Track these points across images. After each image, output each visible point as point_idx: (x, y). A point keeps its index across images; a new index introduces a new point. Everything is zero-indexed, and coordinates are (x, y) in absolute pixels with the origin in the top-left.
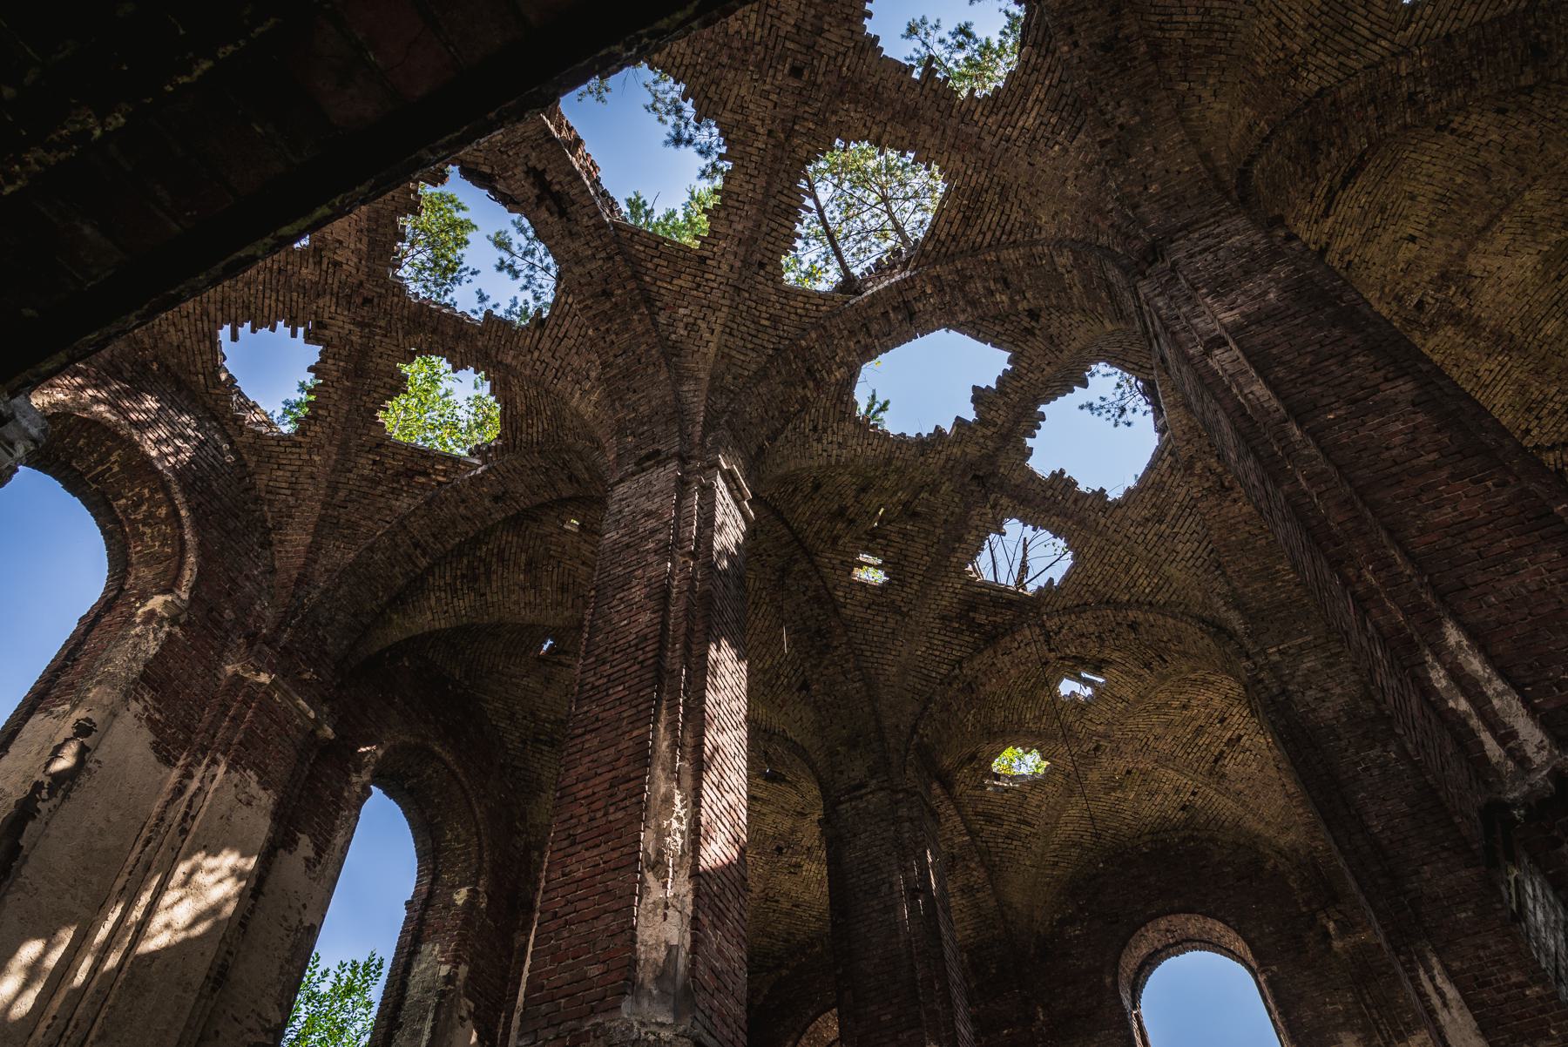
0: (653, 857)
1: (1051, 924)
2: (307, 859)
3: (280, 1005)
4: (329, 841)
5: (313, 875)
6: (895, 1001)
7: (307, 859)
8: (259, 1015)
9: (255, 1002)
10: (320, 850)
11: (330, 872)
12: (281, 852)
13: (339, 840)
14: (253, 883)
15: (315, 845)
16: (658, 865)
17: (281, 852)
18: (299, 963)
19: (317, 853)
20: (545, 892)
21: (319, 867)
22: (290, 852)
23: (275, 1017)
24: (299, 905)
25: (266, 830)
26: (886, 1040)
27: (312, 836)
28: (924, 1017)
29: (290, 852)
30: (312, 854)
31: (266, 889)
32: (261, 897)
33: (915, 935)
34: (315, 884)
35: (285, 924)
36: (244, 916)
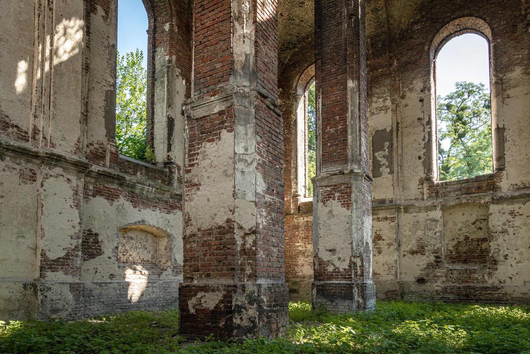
0: (237, 14)
1: (408, 25)
2: (103, 17)
3: (112, 76)
4: (109, 7)
5: (107, 23)
6: (337, 63)
7: (103, 17)
8: (105, 80)
9: (103, 76)
10: (107, 12)
11: (113, 21)
12: (92, 14)
13: (112, 7)
14: (85, 29)
15: (104, 10)
16: (239, 18)
17: (92, 14)
18: (114, 60)
19: (106, 14)
20: (195, 33)
21: (108, 20)
22: (95, 14)
23: (112, 81)
24: (106, 37)
25: (82, 5)
26: (332, 79)
27: (101, 5)
28: (348, 69)
29: (95, 14)
30: (104, 14)
31: (91, 31)
32: (91, 35)
33: (348, 35)
34: (109, 27)
35: (103, 45)
36: (87, 43)
